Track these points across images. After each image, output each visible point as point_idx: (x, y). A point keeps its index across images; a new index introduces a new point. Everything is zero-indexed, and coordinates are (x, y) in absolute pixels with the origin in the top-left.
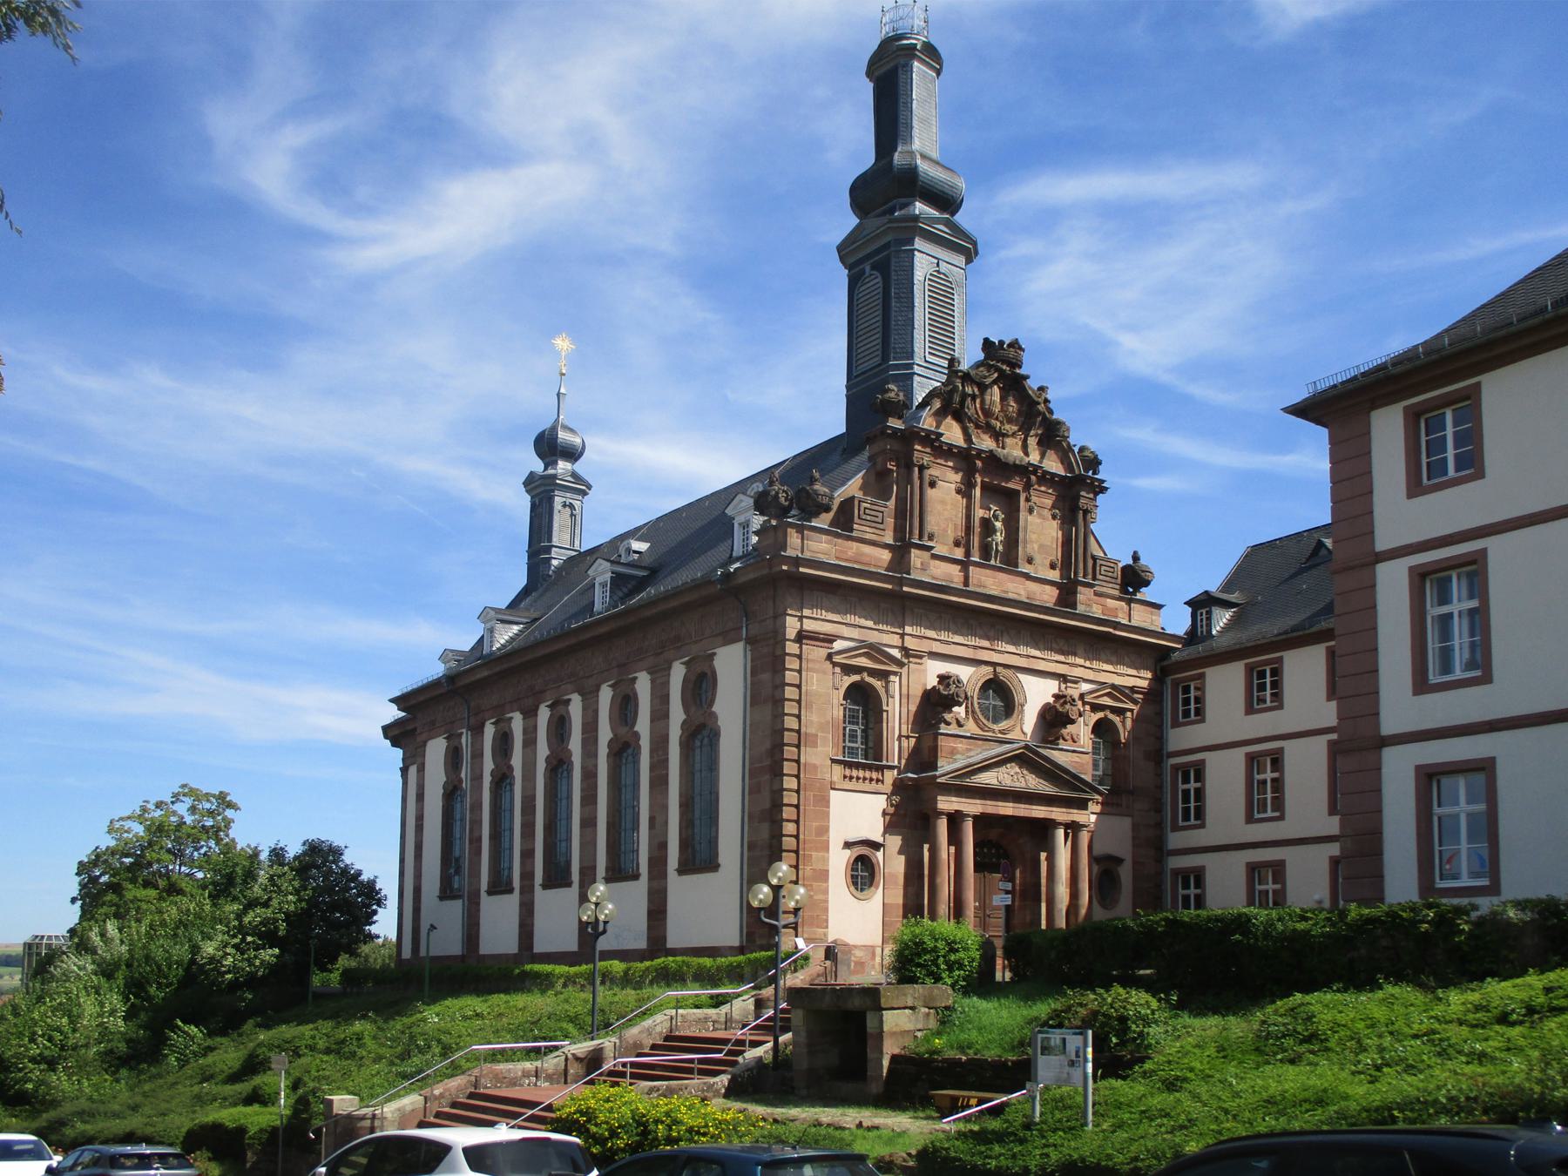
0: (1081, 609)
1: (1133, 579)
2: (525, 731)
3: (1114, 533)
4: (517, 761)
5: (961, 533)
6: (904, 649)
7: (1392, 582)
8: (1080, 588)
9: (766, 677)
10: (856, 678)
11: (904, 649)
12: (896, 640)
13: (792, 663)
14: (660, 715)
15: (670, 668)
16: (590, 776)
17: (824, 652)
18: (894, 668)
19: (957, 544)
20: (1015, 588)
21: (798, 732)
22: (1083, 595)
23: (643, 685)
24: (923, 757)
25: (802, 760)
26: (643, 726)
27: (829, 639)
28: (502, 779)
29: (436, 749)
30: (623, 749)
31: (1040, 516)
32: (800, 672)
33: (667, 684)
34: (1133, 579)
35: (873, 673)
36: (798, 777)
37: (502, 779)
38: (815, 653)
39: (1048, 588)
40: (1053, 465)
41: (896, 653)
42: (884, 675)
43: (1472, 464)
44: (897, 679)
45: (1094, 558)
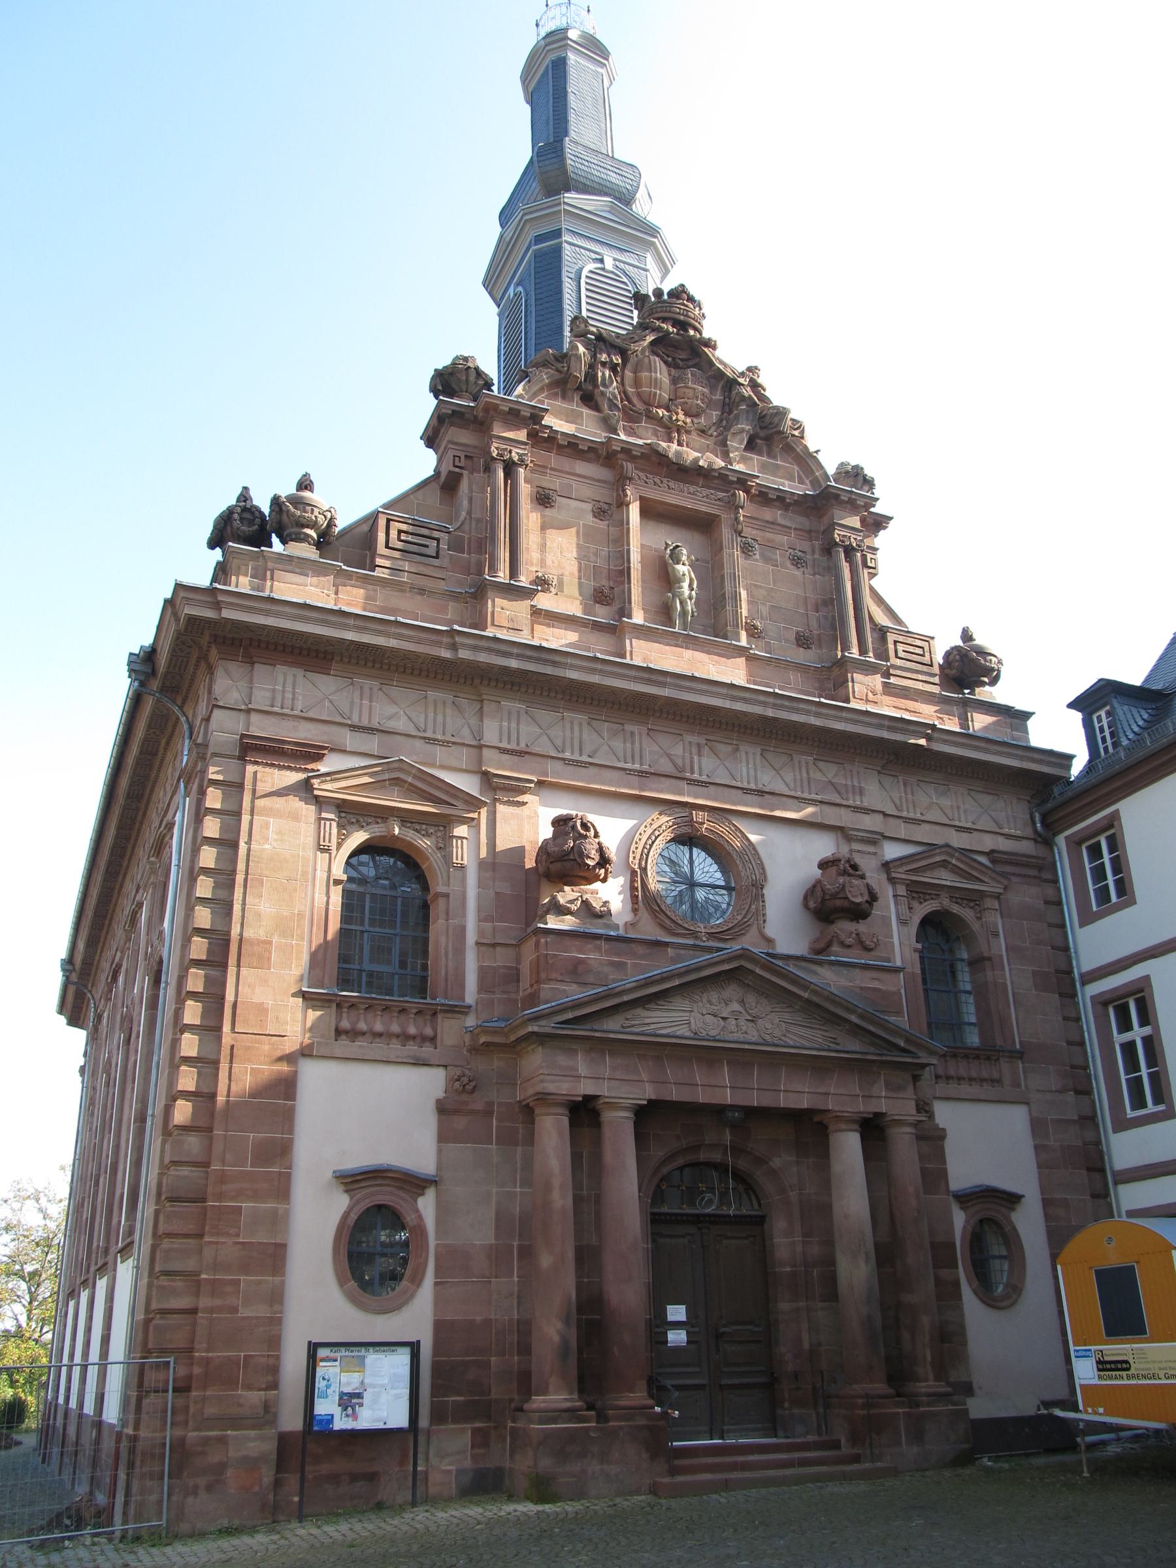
1: (967, 669)
3: (920, 584)
6: (486, 777)
10: (378, 830)
12: (464, 757)
31: (766, 560)
34: (967, 669)
35: (407, 818)
41: (467, 784)
45: (882, 632)
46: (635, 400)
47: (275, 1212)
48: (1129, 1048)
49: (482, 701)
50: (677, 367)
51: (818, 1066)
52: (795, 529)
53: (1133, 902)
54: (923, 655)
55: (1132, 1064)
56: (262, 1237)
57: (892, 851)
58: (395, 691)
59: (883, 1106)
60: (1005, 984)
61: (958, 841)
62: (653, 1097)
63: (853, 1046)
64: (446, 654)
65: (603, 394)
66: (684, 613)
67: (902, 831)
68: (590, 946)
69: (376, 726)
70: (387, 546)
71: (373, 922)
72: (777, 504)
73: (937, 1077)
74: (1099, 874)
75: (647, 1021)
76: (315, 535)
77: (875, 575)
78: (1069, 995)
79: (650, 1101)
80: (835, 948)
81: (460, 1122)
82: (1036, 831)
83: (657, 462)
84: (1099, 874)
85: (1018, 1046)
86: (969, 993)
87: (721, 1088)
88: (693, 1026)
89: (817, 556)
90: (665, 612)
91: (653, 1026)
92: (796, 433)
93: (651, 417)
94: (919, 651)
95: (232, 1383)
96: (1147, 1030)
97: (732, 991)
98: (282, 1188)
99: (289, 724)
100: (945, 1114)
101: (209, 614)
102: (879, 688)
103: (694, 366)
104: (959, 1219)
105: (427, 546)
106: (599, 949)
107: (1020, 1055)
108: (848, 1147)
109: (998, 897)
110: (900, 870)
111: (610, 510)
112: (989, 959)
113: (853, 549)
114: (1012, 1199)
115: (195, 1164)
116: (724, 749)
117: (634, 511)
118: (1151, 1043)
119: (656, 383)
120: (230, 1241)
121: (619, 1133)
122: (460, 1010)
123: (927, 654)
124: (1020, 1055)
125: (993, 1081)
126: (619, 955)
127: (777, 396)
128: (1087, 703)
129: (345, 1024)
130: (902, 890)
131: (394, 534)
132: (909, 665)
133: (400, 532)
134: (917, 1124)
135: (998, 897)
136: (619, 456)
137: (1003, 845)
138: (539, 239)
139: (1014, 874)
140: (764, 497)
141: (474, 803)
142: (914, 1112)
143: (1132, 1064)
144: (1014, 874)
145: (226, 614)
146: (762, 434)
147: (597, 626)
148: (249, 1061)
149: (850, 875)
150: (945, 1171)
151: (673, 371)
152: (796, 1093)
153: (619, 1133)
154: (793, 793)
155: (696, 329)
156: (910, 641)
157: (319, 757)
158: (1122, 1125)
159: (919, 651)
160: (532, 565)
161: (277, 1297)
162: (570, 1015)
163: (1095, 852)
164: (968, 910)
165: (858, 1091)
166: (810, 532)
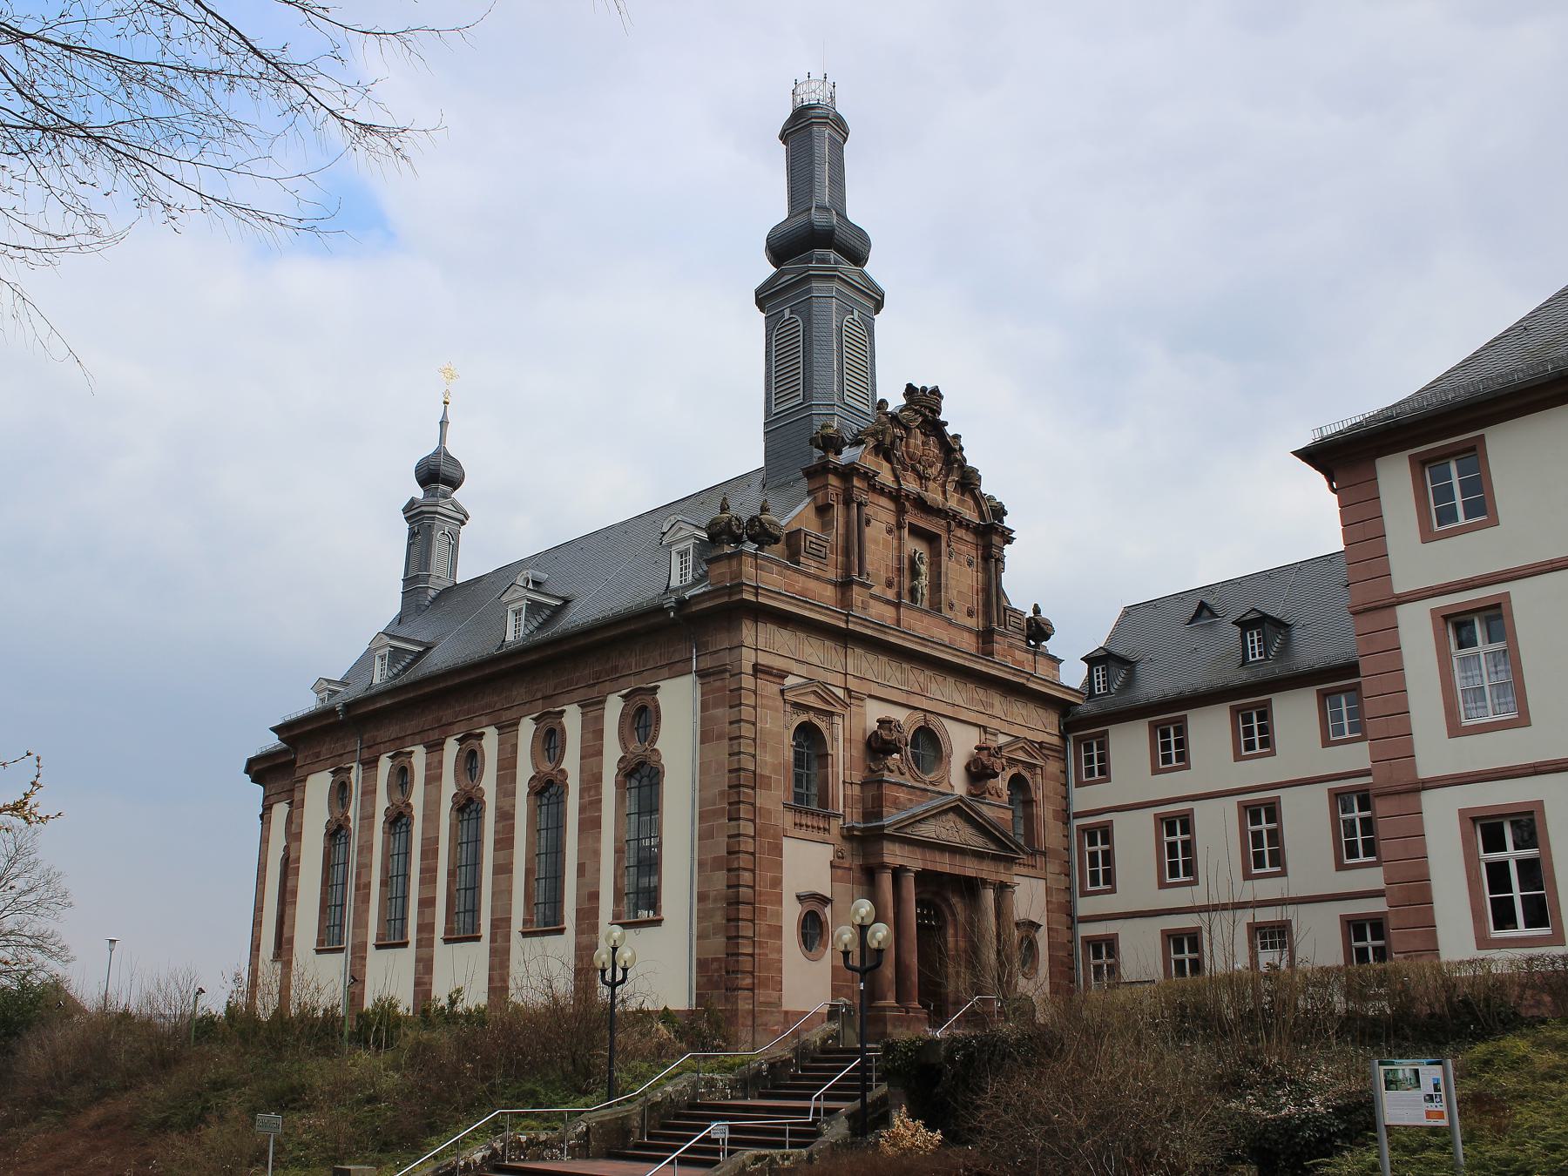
0: (997, 658)
1: (1038, 630)
2: (428, 767)
3: (1025, 579)
4: (417, 799)
6: (848, 691)
7: (1416, 629)
9: (722, 713)
11: (848, 691)
12: (839, 679)
13: (748, 699)
14: (592, 752)
15: (603, 702)
16: (505, 817)
17: (776, 688)
18: (838, 709)
19: (889, 584)
20: (940, 633)
22: (999, 645)
23: (572, 720)
26: (571, 762)
27: (782, 675)
28: (398, 820)
29: (318, 786)
30: (547, 790)
31: (958, 562)
32: (755, 708)
33: (600, 719)
36: (754, 821)
37: (398, 820)
38: (770, 688)
39: (966, 635)
40: (970, 515)
41: (840, 693)
43: (1482, 508)
44: (840, 721)
48: (1093, 855)
51: (979, 855)
53: (1108, 780)
55: (1094, 863)
58: (812, 641)
59: (1004, 878)
61: (1030, 735)
63: (992, 848)
64: (843, 625)
74: (1090, 760)
78: (1066, 822)
81: (840, 872)
83: (921, 505)
84: (1090, 760)
87: (944, 864)
93: (914, 470)
95: (767, 987)
96: (1106, 847)
97: (951, 816)
101: (753, 599)
107: (1044, 854)
108: (989, 895)
114: (1035, 926)
116: (940, 679)
118: (1108, 857)
119: (916, 446)
122: (837, 816)
124: (1044, 854)
128: (1091, 660)
137: (1048, 739)
143: (1094, 863)
145: (761, 599)
147: (888, 602)
152: (970, 868)
158: (1084, 894)
161: (780, 951)
163: (1089, 748)
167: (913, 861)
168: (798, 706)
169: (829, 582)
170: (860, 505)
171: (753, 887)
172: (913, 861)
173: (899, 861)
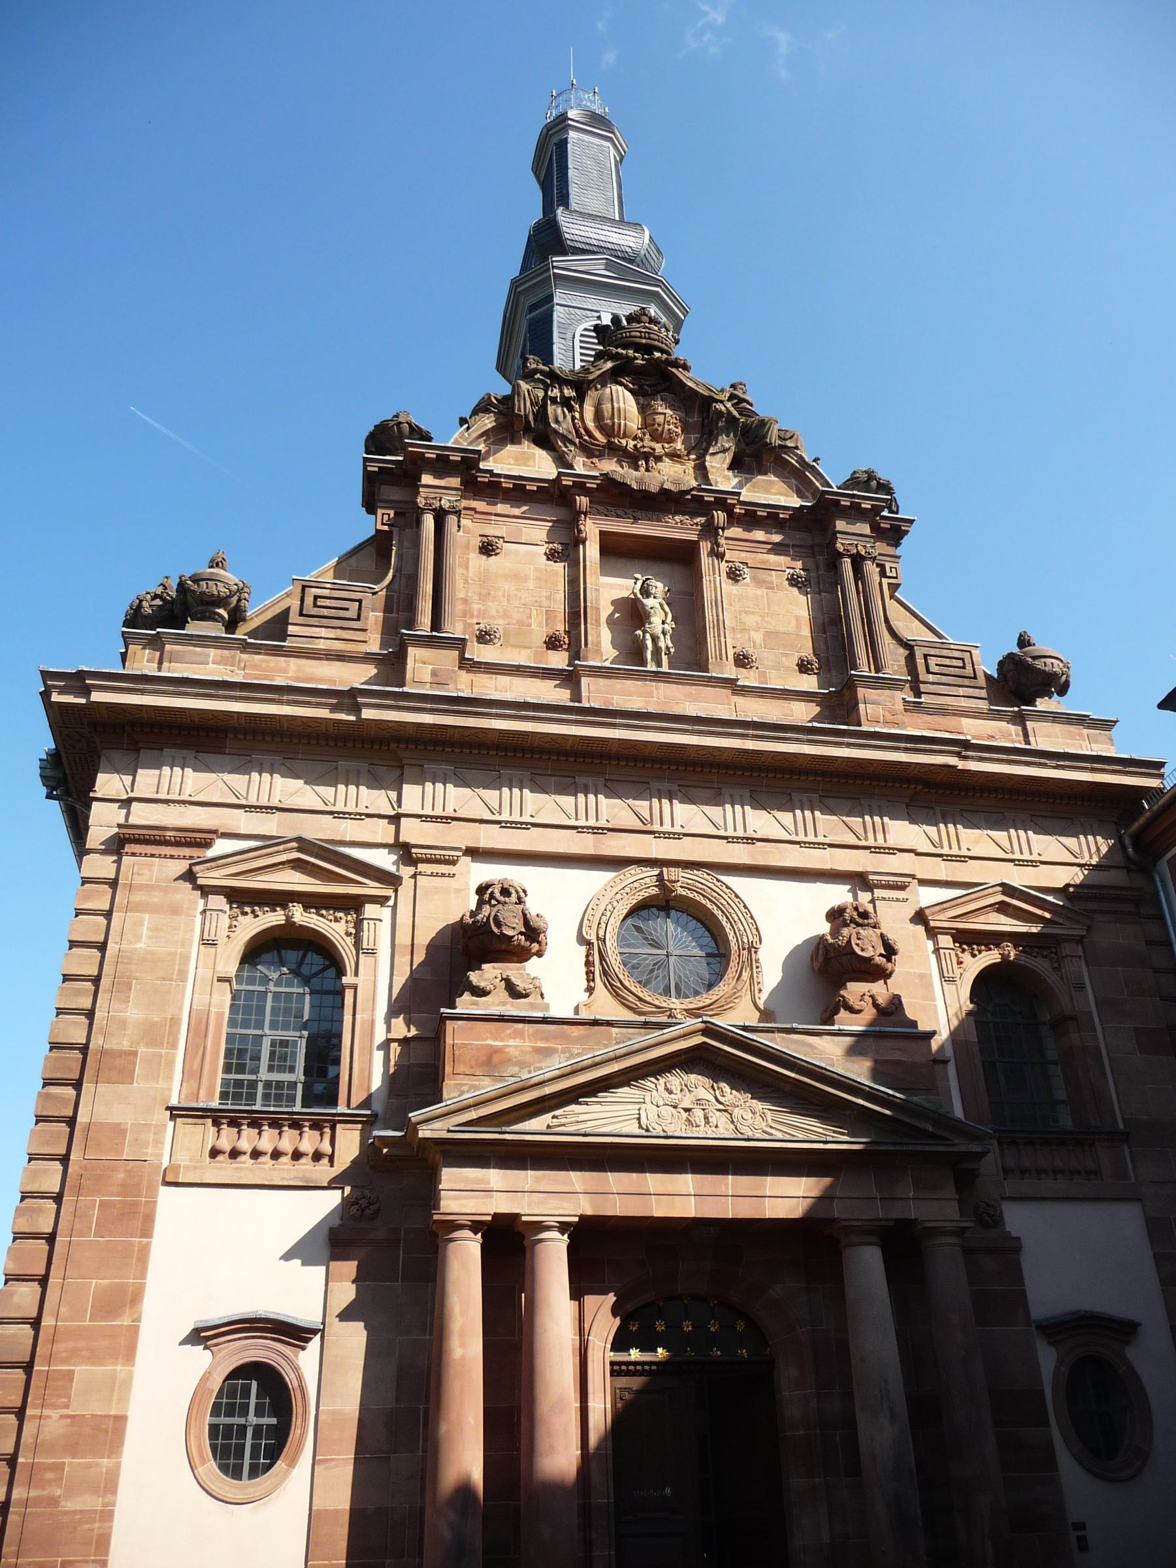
5: (560, 627)
6: (405, 852)
8: (861, 692)
12: (382, 831)
18: (372, 888)
19: (552, 643)
21: (84, 1049)
24: (419, 1075)
25: (82, 1118)
27: (199, 839)
35: (312, 901)
38: (155, 870)
41: (384, 860)
42: (353, 905)
44: (385, 913)
45: (908, 646)
46: (597, 434)
47: (113, 1376)
49: (402, 767)
50: (645, 395)
52: (793, 546)
54: (964, 667)
56: (95, 1408)
57: (928, 897)
60: (1098, 1049)
62: (589, 1212)
65: (555, 431)
66: (657, 651)
67: (942, 871)
68: (509, 1031)
69: (275, 802)
70: (301, 614)
71: (274, 1026)
72: (769, 522)
73: (1006, 1171)
75: (582, 1118)
76: (226, 616)
77: (898, 585)
79: (582, 1217)
80: (843, 1014)
82: (1129, 859)
85: (1121, 1126)
86: (1055, 1063)
88: (644, 1121)
89: (822, 572)
90: (633, 652)
91: (589, 1124)
92: (790, 444)
94: (960, 663)
98: (125, 1347)
99: (173, 808)
100: (1018, 1219)
102: (900, 706)
103: (664, 390)
104: (1047, 1358)
105: (347, 609)
106: (521, 1035)
107: (1124, 1137)
109: (1080, 940)
110: (941, 917)
111: (566, 548)
112: (1073, 1018)
113: (863, 558)
114: (1126, 1330)
115: (23, 1321)
117: (592, 551)
120: (55, 1414)
121: (553, 1260)
123: (969, 666)
124: (1124, 1137)
125: (1089, 1172)
126: (547, 1039)
127: (762, 408)
129: (225, 1144)
130: (945, 941)
131: (309, 600)
132: (944, 679)
133: (316, 597)
134: (960, 1232)
135: (1080, 940)
136: (573, 491)
138: (533, 308)
139: (1101, 912)
140: (751, 517)
141: (392, 880)
142: (957, 1216)
144: (1095, 912)
146: (748, 451)
148: (98, 1192)
149: (858, 925)
150: (1023, 1293)
151: (641, 400)
153: (553, 1260)
154: (793, 838)
155: (662, 351)
156: (945, 653)
157: (207, 844)
159: (960, 663)
160: (472, 616)
161: (110, 1485)
162: (473, 1115)
164: (1040, 960)
165: (875, 1193)
166: (812, 547)
167: (553, 1199)
168: (242, 899)
169: (367, 658)
170: (440, 516)
171: (36, 1323)
172: (553, 1199)
173: (503, 1205)
